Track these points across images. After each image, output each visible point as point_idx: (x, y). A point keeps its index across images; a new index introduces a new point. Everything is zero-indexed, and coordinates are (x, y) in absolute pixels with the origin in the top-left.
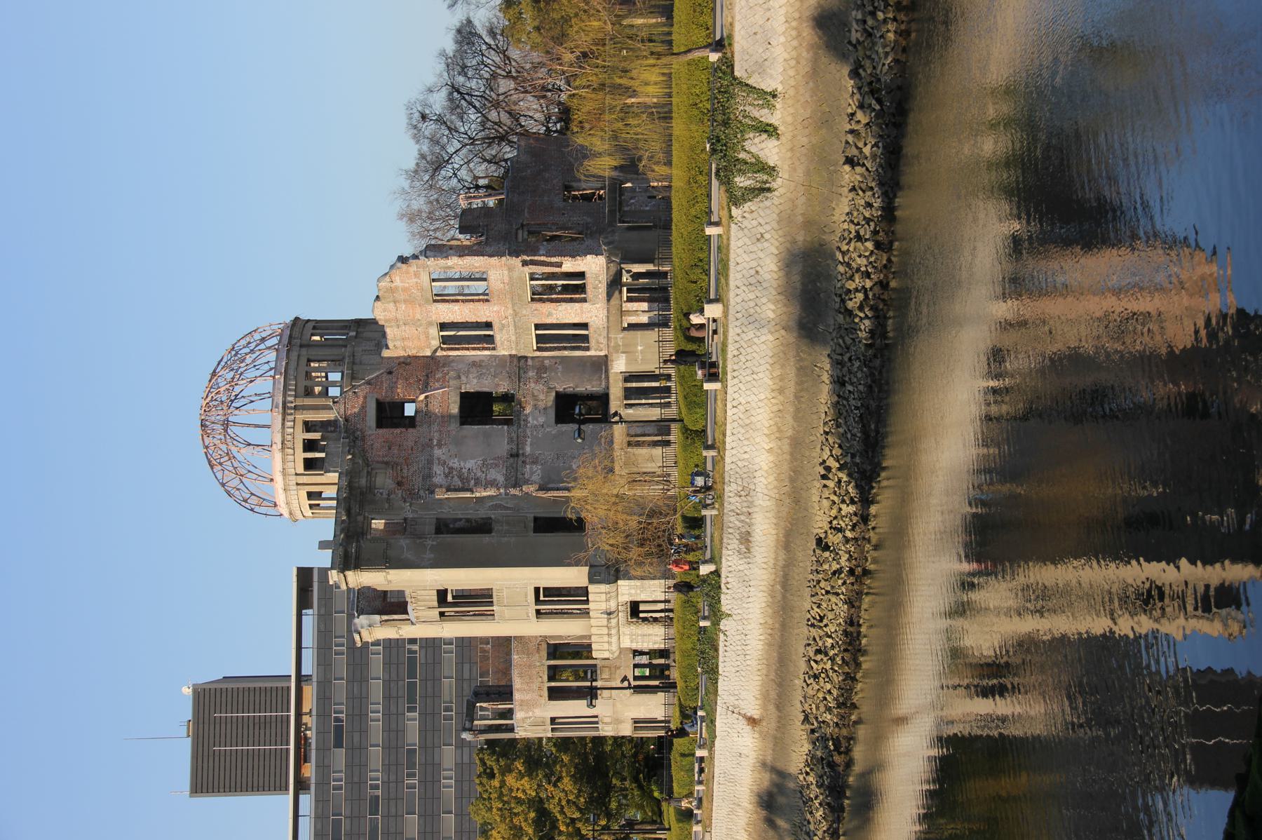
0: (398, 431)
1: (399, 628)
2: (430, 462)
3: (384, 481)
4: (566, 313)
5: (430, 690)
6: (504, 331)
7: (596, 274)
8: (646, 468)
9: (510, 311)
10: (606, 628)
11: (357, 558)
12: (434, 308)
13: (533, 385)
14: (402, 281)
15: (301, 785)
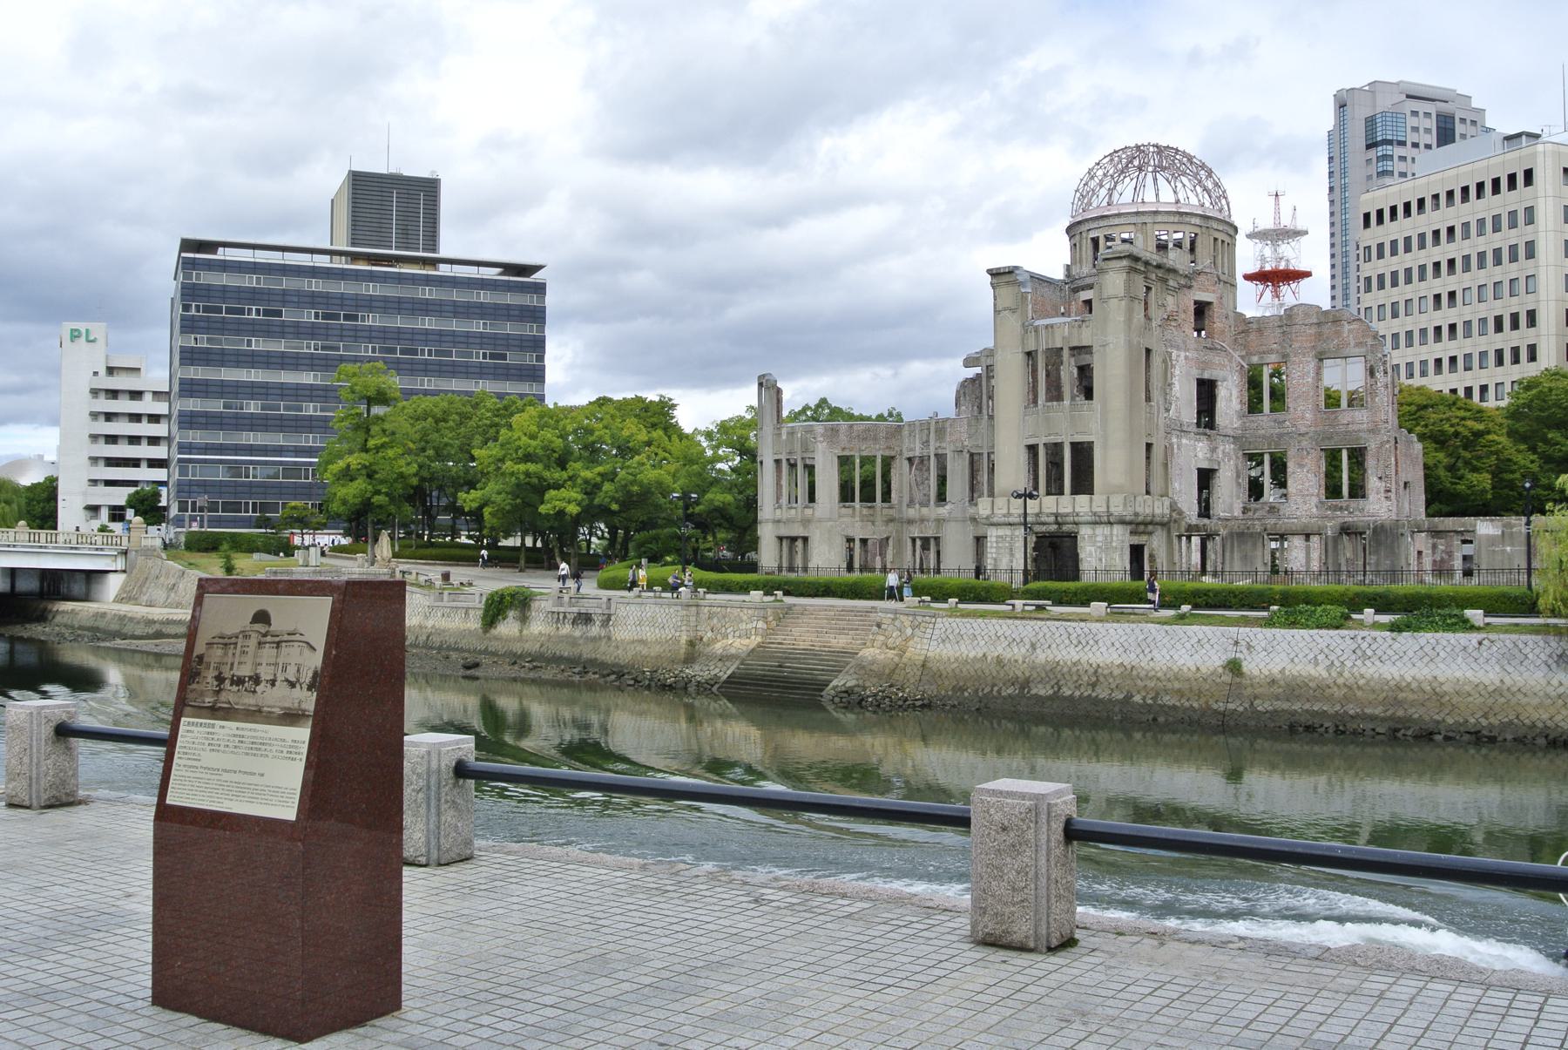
0: (1193, 320)
1: (1013, 311)
2: (1178, 349)
3: (1170, 300)
4: (1305, 479)
5: (444, 368)
6: (1273, 424)
7: (1363, 509)
8: (1232, 552)
9: (1303, 429)
10: (1037, 511)
11: (1137, 270)
12: (1309, 359)
13: (1222, 448)
14: (1349, 331)
15: (355, 257)
